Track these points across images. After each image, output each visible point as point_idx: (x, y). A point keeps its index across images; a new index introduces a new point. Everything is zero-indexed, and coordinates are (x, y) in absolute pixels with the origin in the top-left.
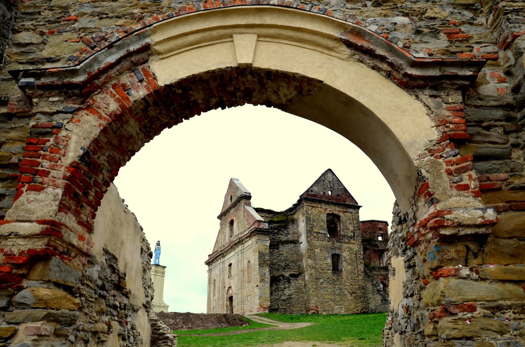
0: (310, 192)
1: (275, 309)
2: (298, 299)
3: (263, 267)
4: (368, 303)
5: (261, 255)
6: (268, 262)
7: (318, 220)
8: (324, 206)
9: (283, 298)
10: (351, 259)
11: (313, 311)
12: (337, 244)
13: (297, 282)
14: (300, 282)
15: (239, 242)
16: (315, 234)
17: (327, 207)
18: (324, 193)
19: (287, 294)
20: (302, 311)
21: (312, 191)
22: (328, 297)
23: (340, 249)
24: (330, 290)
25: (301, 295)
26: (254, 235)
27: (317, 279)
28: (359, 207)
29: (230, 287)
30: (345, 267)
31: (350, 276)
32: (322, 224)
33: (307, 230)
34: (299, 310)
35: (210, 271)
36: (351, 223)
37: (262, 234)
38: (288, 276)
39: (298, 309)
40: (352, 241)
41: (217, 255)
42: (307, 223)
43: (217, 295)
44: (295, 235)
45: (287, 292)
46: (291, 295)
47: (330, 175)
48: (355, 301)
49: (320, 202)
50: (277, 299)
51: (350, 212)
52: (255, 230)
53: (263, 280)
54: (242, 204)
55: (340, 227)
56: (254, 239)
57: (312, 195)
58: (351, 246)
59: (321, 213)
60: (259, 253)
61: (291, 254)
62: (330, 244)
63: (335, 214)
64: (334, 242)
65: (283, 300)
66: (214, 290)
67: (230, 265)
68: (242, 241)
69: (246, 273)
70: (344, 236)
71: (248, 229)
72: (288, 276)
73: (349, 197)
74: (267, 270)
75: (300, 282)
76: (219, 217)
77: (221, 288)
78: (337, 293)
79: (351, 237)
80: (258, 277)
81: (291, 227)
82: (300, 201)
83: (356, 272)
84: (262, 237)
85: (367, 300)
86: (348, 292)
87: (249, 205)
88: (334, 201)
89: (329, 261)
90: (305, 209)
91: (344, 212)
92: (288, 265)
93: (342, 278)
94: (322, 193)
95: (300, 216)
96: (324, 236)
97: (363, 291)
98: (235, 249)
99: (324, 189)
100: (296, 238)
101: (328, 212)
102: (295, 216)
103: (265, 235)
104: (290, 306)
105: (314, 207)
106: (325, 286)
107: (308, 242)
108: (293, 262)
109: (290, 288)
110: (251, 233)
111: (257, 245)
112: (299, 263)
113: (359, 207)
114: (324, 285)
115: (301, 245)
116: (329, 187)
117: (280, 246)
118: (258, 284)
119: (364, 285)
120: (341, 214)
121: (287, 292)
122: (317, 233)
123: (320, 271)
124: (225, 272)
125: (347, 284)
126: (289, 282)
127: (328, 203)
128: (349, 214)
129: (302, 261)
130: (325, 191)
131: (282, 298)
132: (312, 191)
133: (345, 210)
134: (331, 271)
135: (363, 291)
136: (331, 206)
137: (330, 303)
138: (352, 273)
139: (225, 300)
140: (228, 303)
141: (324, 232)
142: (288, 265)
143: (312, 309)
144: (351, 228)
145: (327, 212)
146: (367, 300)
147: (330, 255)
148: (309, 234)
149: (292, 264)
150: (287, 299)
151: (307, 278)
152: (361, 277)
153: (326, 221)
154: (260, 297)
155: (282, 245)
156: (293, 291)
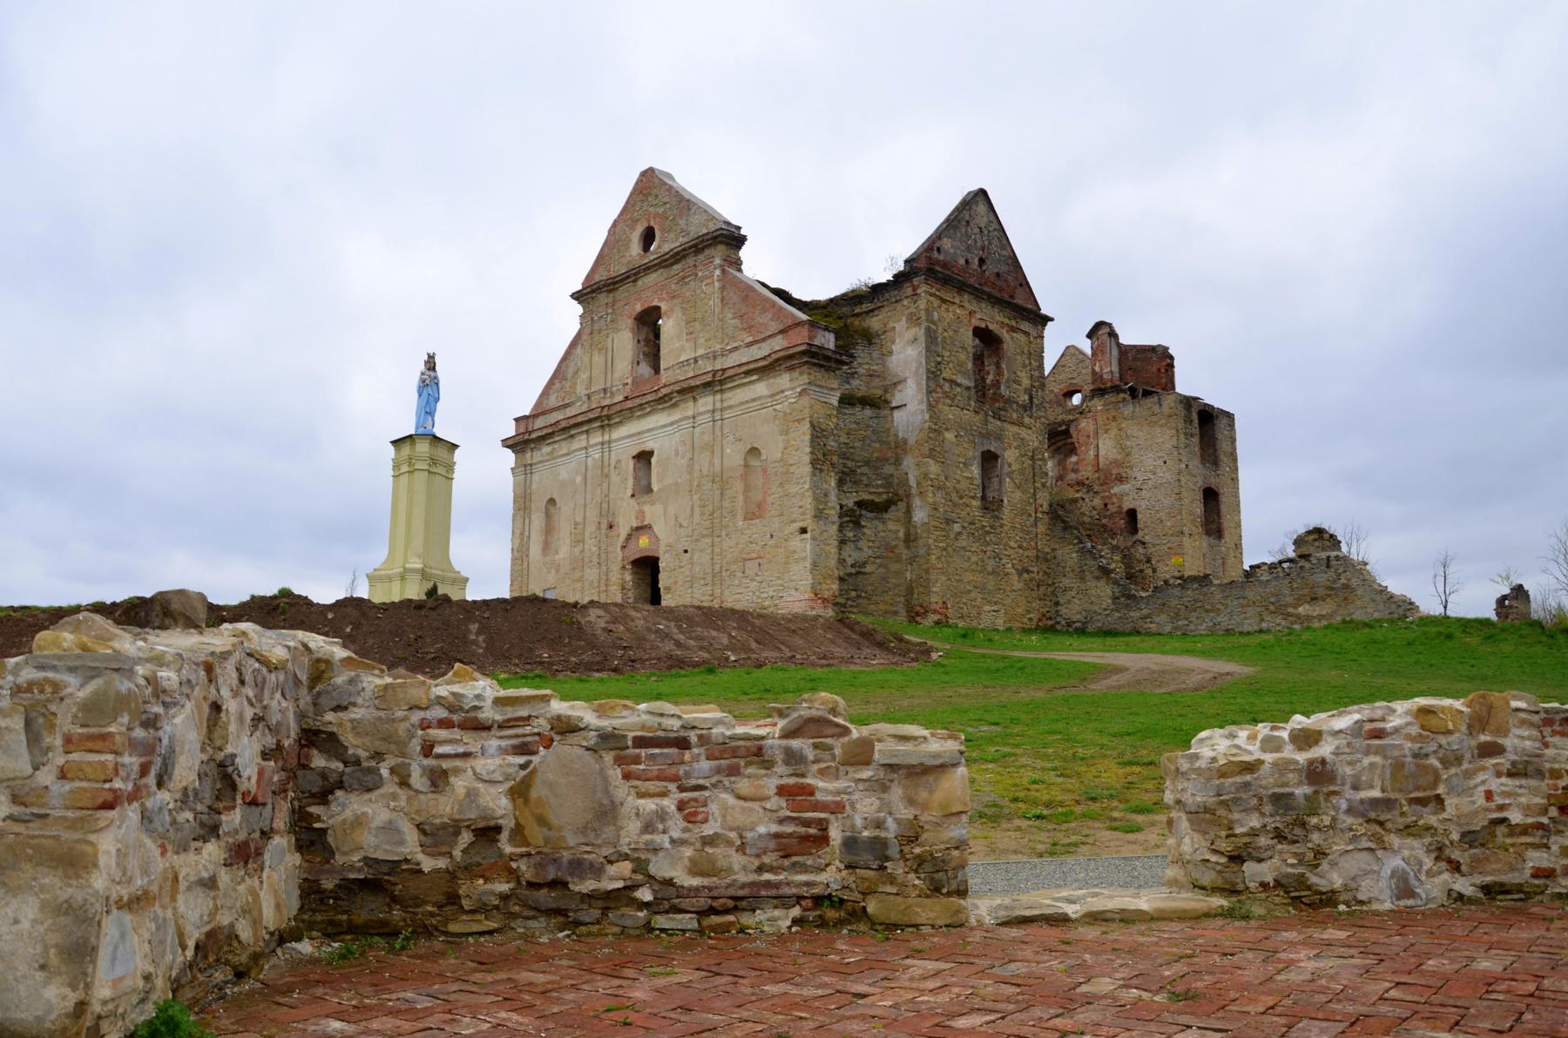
0: (935, 254)
2: (885, 579)
3: (821, 471)
4: (1057, 604)
5: (818, 434)
6: (835, 459)
10: (1022, 471)
11: (936, 617)
13: (881, 527)
14: (891, 526)
15: (707, 385)
16: (947, 387)
17: (973, 306)
19: (850, 561)
20: (896, 613)
21: (939, 250)
22: (968, 577)
23: (999, 438)
24: (974, 559)
25: (894, 567)
26: (791, 369)
28: (1046, 319)
29: (641, 529)
32: (963, 357)
33: (928, 371)
35: (523, 470)
36: (1024, 366)
37: (821, 366)
38: (851, 504)
39: (882, 606)
40: (1027, 420)
41: (580, 419)
42: (928, 349)
43: (564, 551)
44: (876, 382)
47: (981, 208)
49: (962, 287)
52: (803, 353)
53: (821, 511)
54: (718, 261)
55: (999, 372)
56: (784, 380)
58: (1024, 433)
60: (813, 426)
61: (863, 440)
62: (978, 419)
66: (549, 529)
67: (644, 457)
68: (721, 382)
69: (738, 486)
70: (1009, 401)
71: (750, 345)
72: (851, 504)
74: (833, 483)
75: (891, 526)
76: (577, 296)
77: (590, 528)
79: (1025, 408)
80: (808, 503)
82: (900, 279)
83: (1031, 509)
84: (819, 375)
85: (1053, 593)
87: (737, 264)
88: (994, 292)
89: (975, 470)
90: (922, 304)
92: (853, 472)
94: (962, 261)
95: (901, 325)
96: (966, 393)
98: (675, 405)
99: (968, 249)
100: (879, 392)
102: (874, 323)
103: (828, 369)
105: (944, 301)
106: (964, 543)
107: (930, 407)
108: (867, 463)
109: (860, 544)
110: (777, 360)
111: (806, 401)
112: (888, 469)
113: (1046, 319)
114: (963, 542)
115: (896, 414)
118: (808, 522)
120: (1005, 335)
122: (952, 382)
123: (956, 499)
124: (615, 478)
125: (1012, 544)
126: (857, 524)
127: (979, 294)
128: (1023, 338)
129: (898, 462)
130: (969, 256)
138: (1023, 512)
139: (616, 567)
140: (628, 577)
142: (853, 472)
143: (935, 612)
144: (1026, 382)
145: (975, 322)
146: (1053, 593)
147: (978, 454)
148: (932, 384)
149: (865, 470)
150: (850, 575)
151: (919, 516)
152: (1041, 528)
153: (971, 350)
154: (815, 565)
156: (870, 552)
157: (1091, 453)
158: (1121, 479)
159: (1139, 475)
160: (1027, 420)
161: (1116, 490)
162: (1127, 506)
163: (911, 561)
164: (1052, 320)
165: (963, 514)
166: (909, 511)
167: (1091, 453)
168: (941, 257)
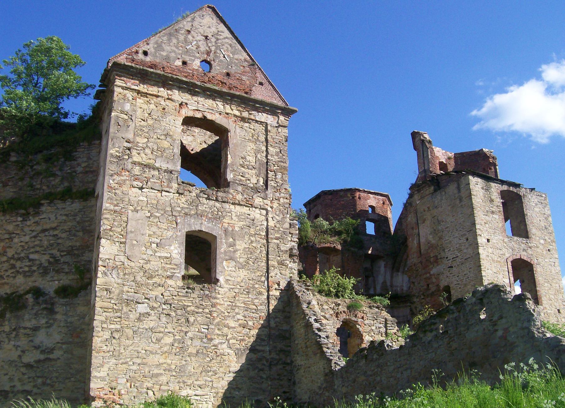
0: (141, 56)
7: (152, 128)
8: (176, 95)
12: (206, 205)
16: (137, 170)
18: (184, 63)
24: (168, 340)
27: (128, 302)
30: (226, 270)
31: (242, 297)
38: (52, 294)
40: (258, 201)
46: (52, 350)
48: (252, 373)
49: (167, 82)
51: (261, 123)
57: (142, 63)
58: (256, 214)
63: (212, 121)
64: (198, 196)
65: (29, 366)
72: (52, 294)
73: (261, 84)
78: (193, 350)
79: (256, 190)
81: (81, 154)
89: (177, 251)
91: (243, 119)
92: (57, 261)
93: (214, 305)
94: (179, 63)
97: (280, 345)
101: (190, 114)
104: (44, 384)
105: (146, 95)
106: (152, 324)
108: (70, 252)
114: (149, 323)
116: (203, 48)
117: (43, 209)
119: (285, 327)
123: (140, 277)
125: (232, 324)
126: (51, 311)
127: (191, 88)
130: (187, 59)
131: (27, 359)
132: (145, 53)
133: (245, 114)
134: (180, 283)
135: (280, 345)
136: (201, 99)
137: (164, 379)
141: (171, 167)
145: (187, 112)
149: (68, 259)
150: (39, 361)
155: (49, 204)
156: (57, 337)
157: (415, 242)
158: (437, 260)
159: (450, 257)
160: (258, 201)
161: (434, 271)
162: (443, 284)
164: (296, 111)
167: (415, 242)
168: (148, 59)
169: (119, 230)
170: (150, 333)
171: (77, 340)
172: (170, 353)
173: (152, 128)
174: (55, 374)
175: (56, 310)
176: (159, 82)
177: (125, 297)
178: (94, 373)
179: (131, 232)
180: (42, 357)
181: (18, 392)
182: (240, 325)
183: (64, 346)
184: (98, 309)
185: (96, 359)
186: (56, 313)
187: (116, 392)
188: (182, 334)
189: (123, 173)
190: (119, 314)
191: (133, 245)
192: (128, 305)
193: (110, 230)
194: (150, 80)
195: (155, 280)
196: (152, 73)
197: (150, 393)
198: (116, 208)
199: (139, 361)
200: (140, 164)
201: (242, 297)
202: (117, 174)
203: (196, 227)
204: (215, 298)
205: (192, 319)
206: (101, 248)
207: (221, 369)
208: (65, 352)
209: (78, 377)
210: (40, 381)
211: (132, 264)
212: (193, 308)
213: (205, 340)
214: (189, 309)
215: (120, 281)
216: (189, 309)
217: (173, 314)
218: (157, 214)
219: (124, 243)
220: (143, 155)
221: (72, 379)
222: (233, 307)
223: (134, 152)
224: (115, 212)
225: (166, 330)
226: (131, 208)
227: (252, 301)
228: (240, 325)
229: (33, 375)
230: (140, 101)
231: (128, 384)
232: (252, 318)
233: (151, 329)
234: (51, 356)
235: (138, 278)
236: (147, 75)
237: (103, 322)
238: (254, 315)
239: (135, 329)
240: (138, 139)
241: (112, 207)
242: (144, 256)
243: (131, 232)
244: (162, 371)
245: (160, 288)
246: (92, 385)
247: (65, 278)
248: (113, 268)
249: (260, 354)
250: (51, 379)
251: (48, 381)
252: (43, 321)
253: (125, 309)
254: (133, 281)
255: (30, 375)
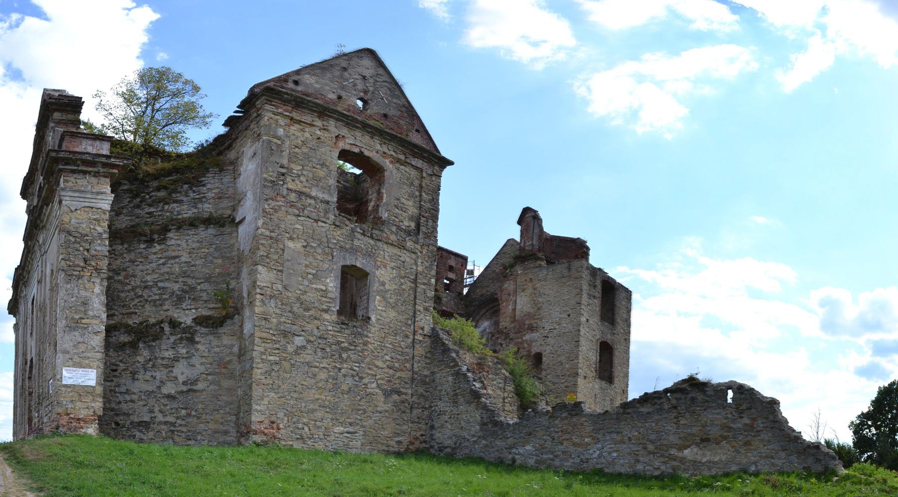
1: (140, 424)
9: (169, 389)
13: (215, 342)
14: (226, 340)
16: (293, 197)
19: (181, 379)
22: (313, 394)
24: (323, 375)
25: (226, 383)
31: (390, 339)
34: (215, 432)
39: (212, 426)
45: (182, 371)
50: (149, 393)
59: (319, 155)
65: (170, 397)
75: (226, 340)
78: (345, 387)
86: (378, 386)
104: (189, 415)
106: (309, 358)
109: (195, 360)
114: (306, 356)
121: (182, 371)
122: (300, 193)
125: (380, 363)
126: (191, 341)
131: (165, 391)
134: (334, 317)
137: (319, 415)
150: (182, 392)
151: (248, 328)
152: (420, 350)
156: (202, 369)
163: (241, 376)
165: (309, 327)
166: (241, 326)
169: (276, 257)
170: (307, 368)
171: (223, 370)
172: (325, 389)
173: (307, 157)
174: (200, 406)
175: (197, 339)
176: (315, 111)
177: (282, 328)
178: (255, 407)
179: (288, 260)
180: (185, 388)
181: (160, 423)
182: (388, 367)
183: (210, 377)
184: (257, 340)
185: (257, 392)
186: (197, 343)
187: (275, 426)
188: (336, 370)
189: (278, 199)
190: (277, 346)
191: (290, 274)
192: (285, 337)
193: (267, 257)
194: (304, 108)
195: (311, 313)
196: (309, 101)
197: (306, 429)
198: (273, 234)
199: (295, 395)
200: (295, 191)
201: (390, 339)
202: (272, 199)
203: (348, 263)
204: (367, 336)
205: (344, 356)
206: (258, 276)
207: (370, 409)
208: (211, 384)
209: (227, 409)
210: (184, 412)
211: (290, 294)
212: (346, 345)
213: (357, 378)
214: (343, 345)
215: (278, 311)
216: (343, 345)
217: (328, 350)
218: (313, 245)
219: (281, 271)
220: (297, 182)
221: (221, 411)
222: (382, 348)
223: (289, 179)
224: (271, 238)
225: (322, 365)
226: (287, 235)
227: (399, 343)
228: (388, 367)
229: (175, 405)
230: (295, 128)
231: (286, 419)
232: (399, 360)
233: (308, 363)
234: (195, 388)
235: (295, 309)
236: (302, 103)
237: (262, 353)
238: (400, 357)
239: (292, 362)
240: (292, 166)
241: (268, 233)
242: (301, 287)
243: (288, 260)
244: (317, 407)
245: (316, 322)
246: (253, 419)
247: (205, 305)
248: (271, 297)
249: (404, 396)
250: (196, 411)
251: (193, 413)
252: (184, 351)
253: (283, 342)
254: (290, 312)
255: (173, 406)
